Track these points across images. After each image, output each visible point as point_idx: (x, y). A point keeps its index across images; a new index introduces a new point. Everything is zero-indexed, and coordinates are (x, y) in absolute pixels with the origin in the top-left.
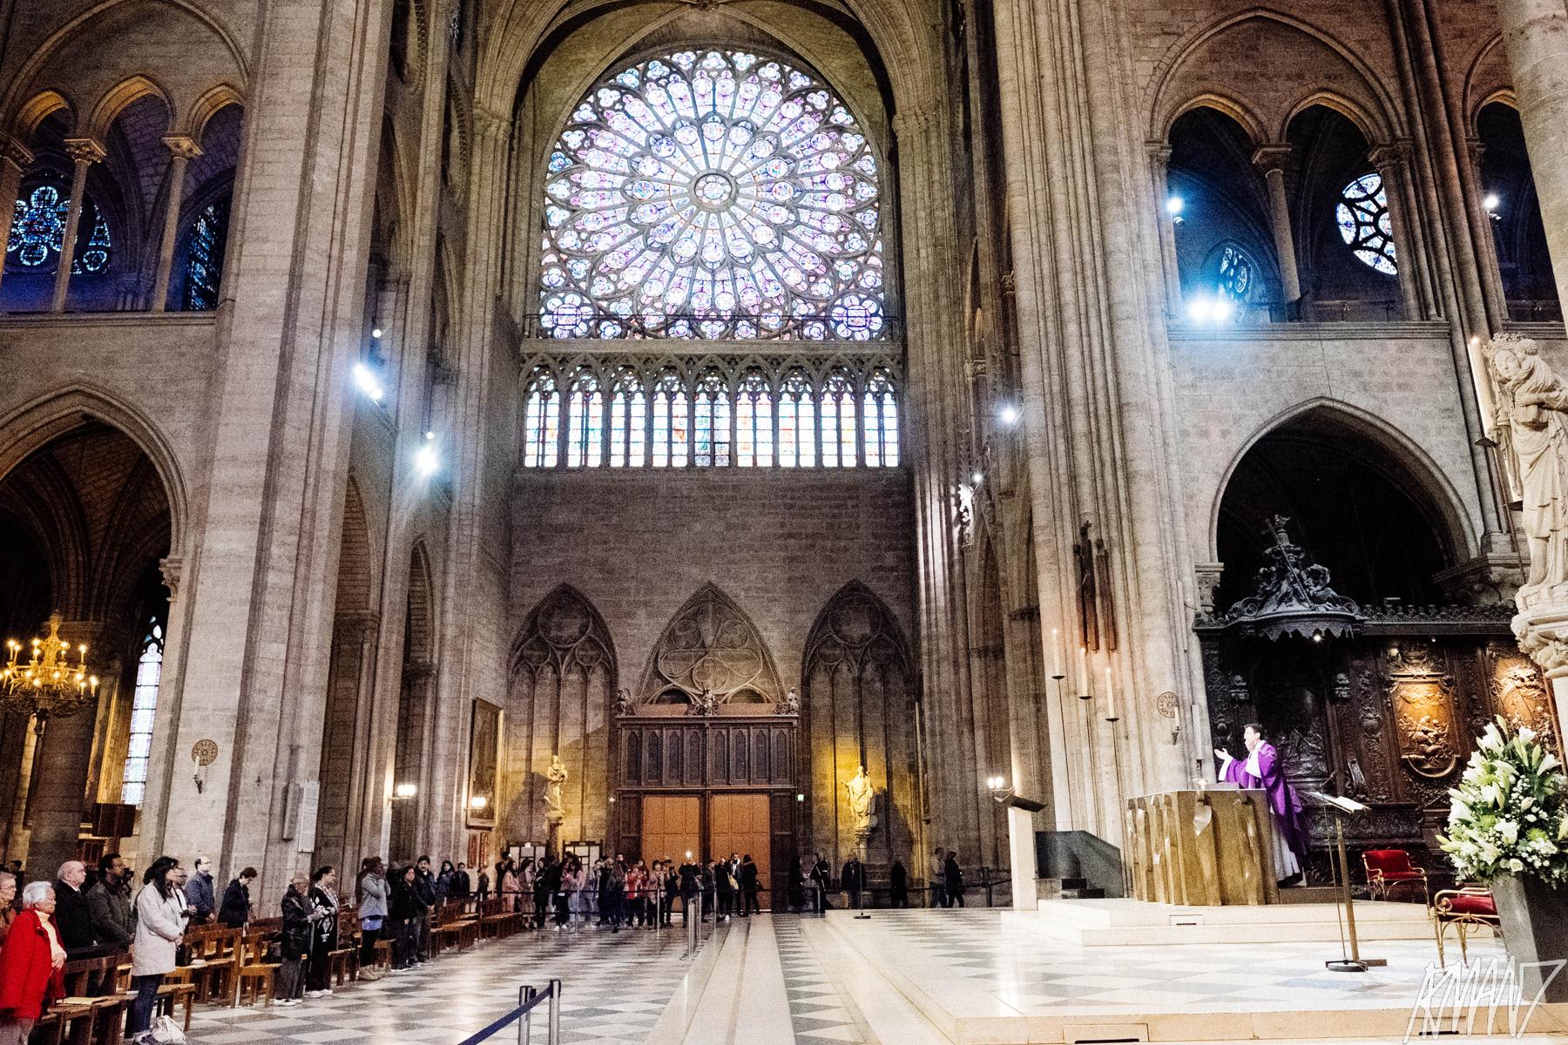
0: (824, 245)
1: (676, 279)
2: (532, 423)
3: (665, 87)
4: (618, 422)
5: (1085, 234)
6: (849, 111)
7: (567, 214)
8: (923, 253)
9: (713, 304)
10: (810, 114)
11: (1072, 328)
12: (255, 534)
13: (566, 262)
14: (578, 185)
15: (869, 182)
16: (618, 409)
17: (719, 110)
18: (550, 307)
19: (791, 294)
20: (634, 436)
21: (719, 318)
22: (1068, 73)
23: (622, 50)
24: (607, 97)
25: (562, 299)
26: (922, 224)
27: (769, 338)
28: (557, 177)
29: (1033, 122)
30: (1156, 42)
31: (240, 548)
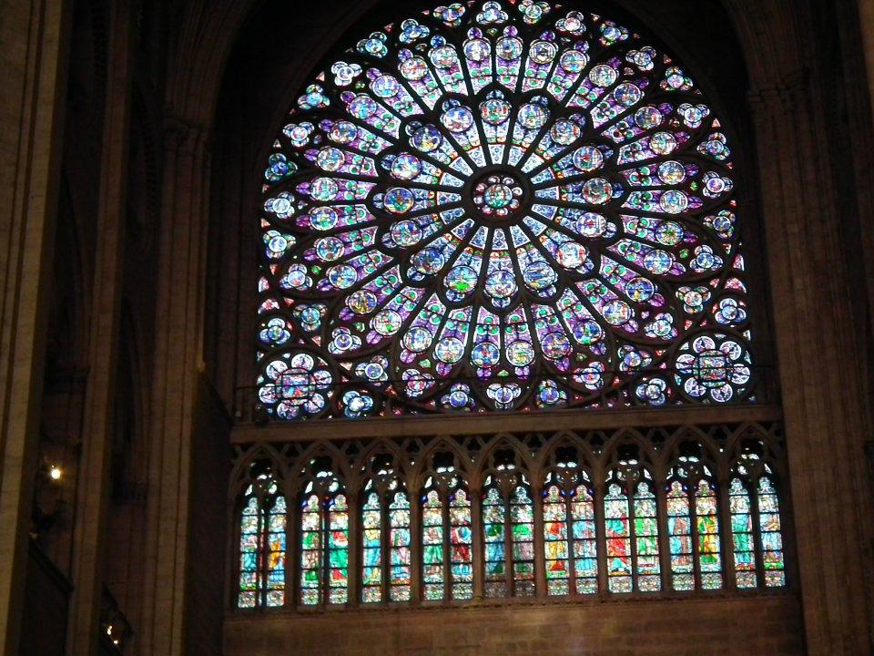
0: (659, 264)
1: (449, 325)
2: (249, 543)
4: (372, 537)
7: (292, 239)
8: (798, 282)
9: (503, 359)
10: (632, 79)
13: (293, 307)
14: (307, 198)
16: (372, 518)
17: (502, 81)
18: (271, 373)
19: (616, 337)
20: (396, 558)
21: (512, 378)
24: (344, 73)
25: (288, 362)
27: (589, 403)
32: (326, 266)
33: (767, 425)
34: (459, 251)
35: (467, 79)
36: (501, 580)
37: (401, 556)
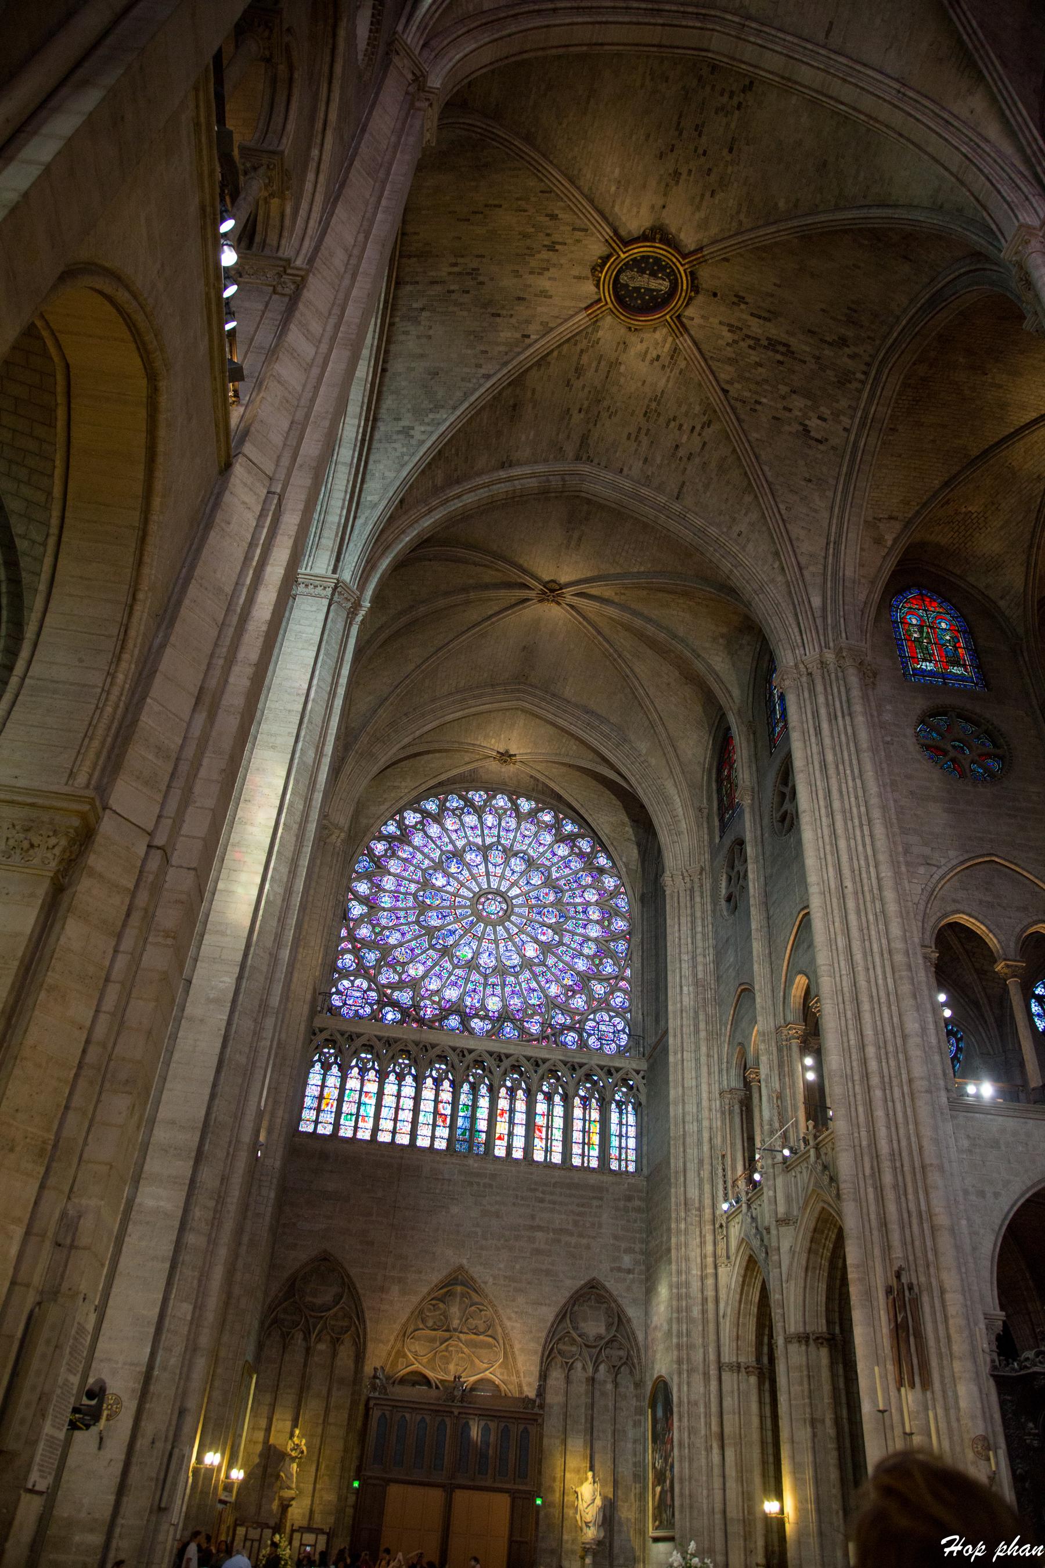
0: (581, 965)
1: (453, 978)
2: (312, 1091)
3: (460, 817)
4: (389, 1101)
5: (886, 1016)
6: (609, 857)
11: (878, 1093)
12: (184, 1194)
15: (623, 917)
16: (390, 1088)
18: (341, 988)
19: (552, 1003)
20: (402, 1115)
22: (866, 888)
23: (432, 783)
24: (411, 818)
25: (352, 982)
26: (685, 965)
28: (360, 877)
29: (837, 919)
30: (922, 870)
31: (166, 1205)
32: (385, 928)
33: (638, 1072)
34: (465, 934)
35: (483, 835)
36: (465, 1141)
37: (406, 1115)
